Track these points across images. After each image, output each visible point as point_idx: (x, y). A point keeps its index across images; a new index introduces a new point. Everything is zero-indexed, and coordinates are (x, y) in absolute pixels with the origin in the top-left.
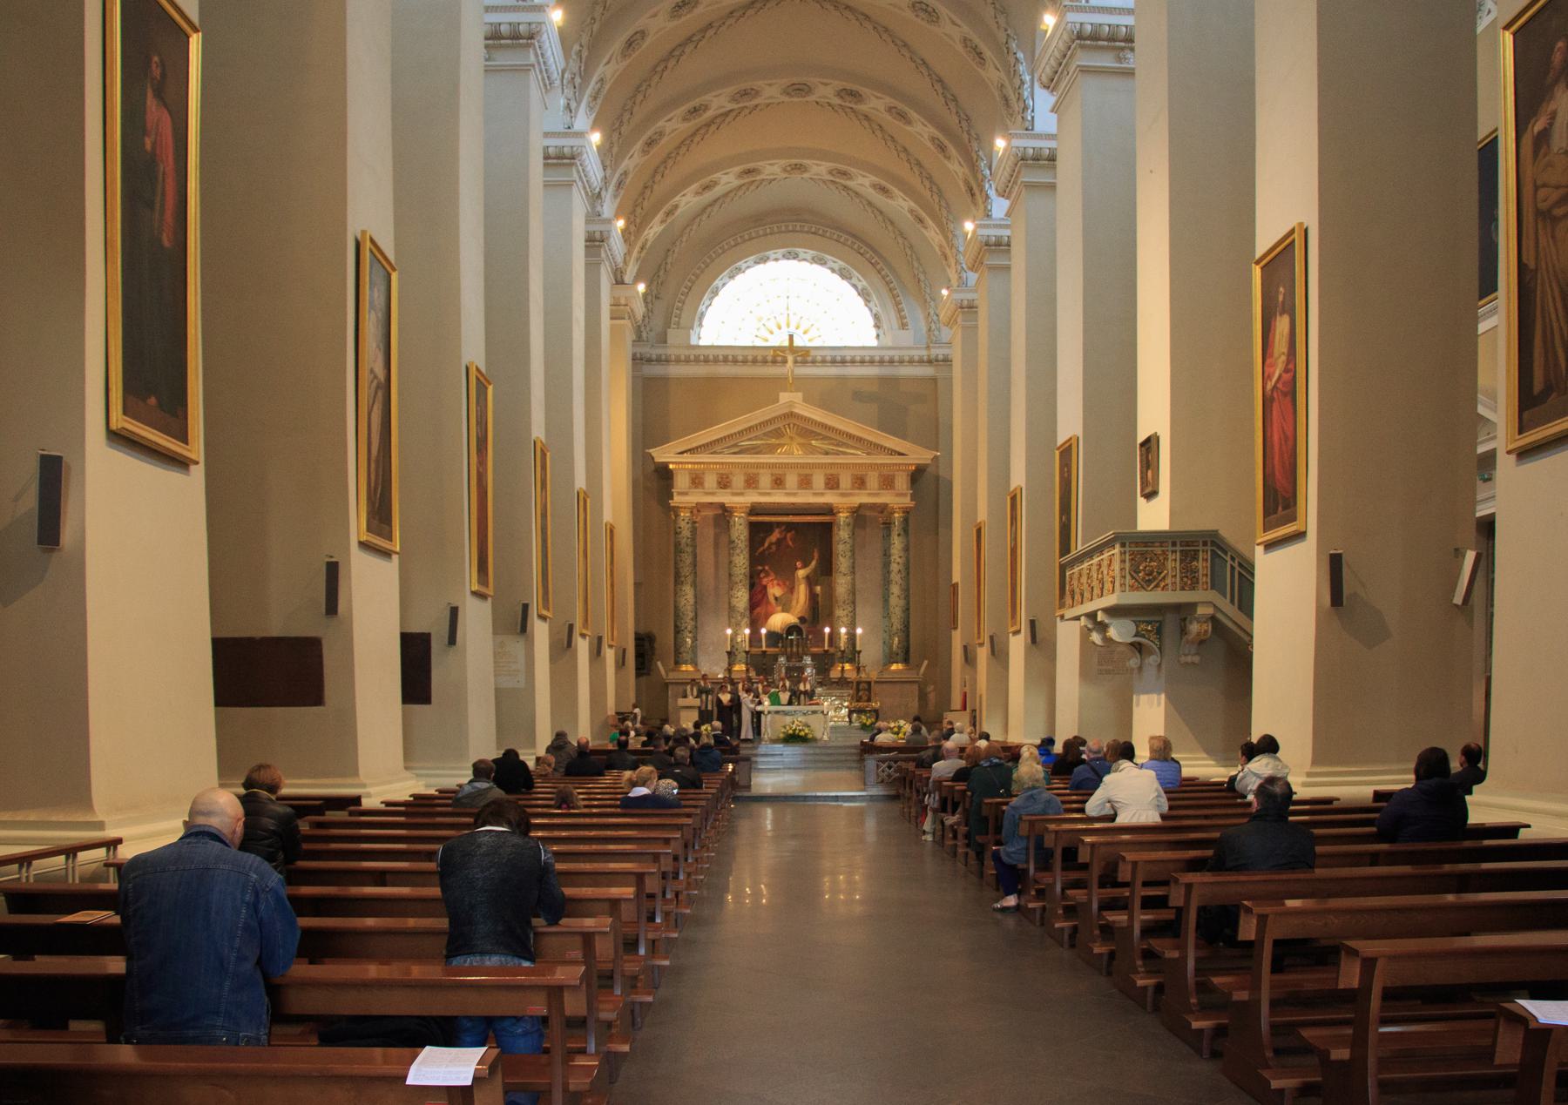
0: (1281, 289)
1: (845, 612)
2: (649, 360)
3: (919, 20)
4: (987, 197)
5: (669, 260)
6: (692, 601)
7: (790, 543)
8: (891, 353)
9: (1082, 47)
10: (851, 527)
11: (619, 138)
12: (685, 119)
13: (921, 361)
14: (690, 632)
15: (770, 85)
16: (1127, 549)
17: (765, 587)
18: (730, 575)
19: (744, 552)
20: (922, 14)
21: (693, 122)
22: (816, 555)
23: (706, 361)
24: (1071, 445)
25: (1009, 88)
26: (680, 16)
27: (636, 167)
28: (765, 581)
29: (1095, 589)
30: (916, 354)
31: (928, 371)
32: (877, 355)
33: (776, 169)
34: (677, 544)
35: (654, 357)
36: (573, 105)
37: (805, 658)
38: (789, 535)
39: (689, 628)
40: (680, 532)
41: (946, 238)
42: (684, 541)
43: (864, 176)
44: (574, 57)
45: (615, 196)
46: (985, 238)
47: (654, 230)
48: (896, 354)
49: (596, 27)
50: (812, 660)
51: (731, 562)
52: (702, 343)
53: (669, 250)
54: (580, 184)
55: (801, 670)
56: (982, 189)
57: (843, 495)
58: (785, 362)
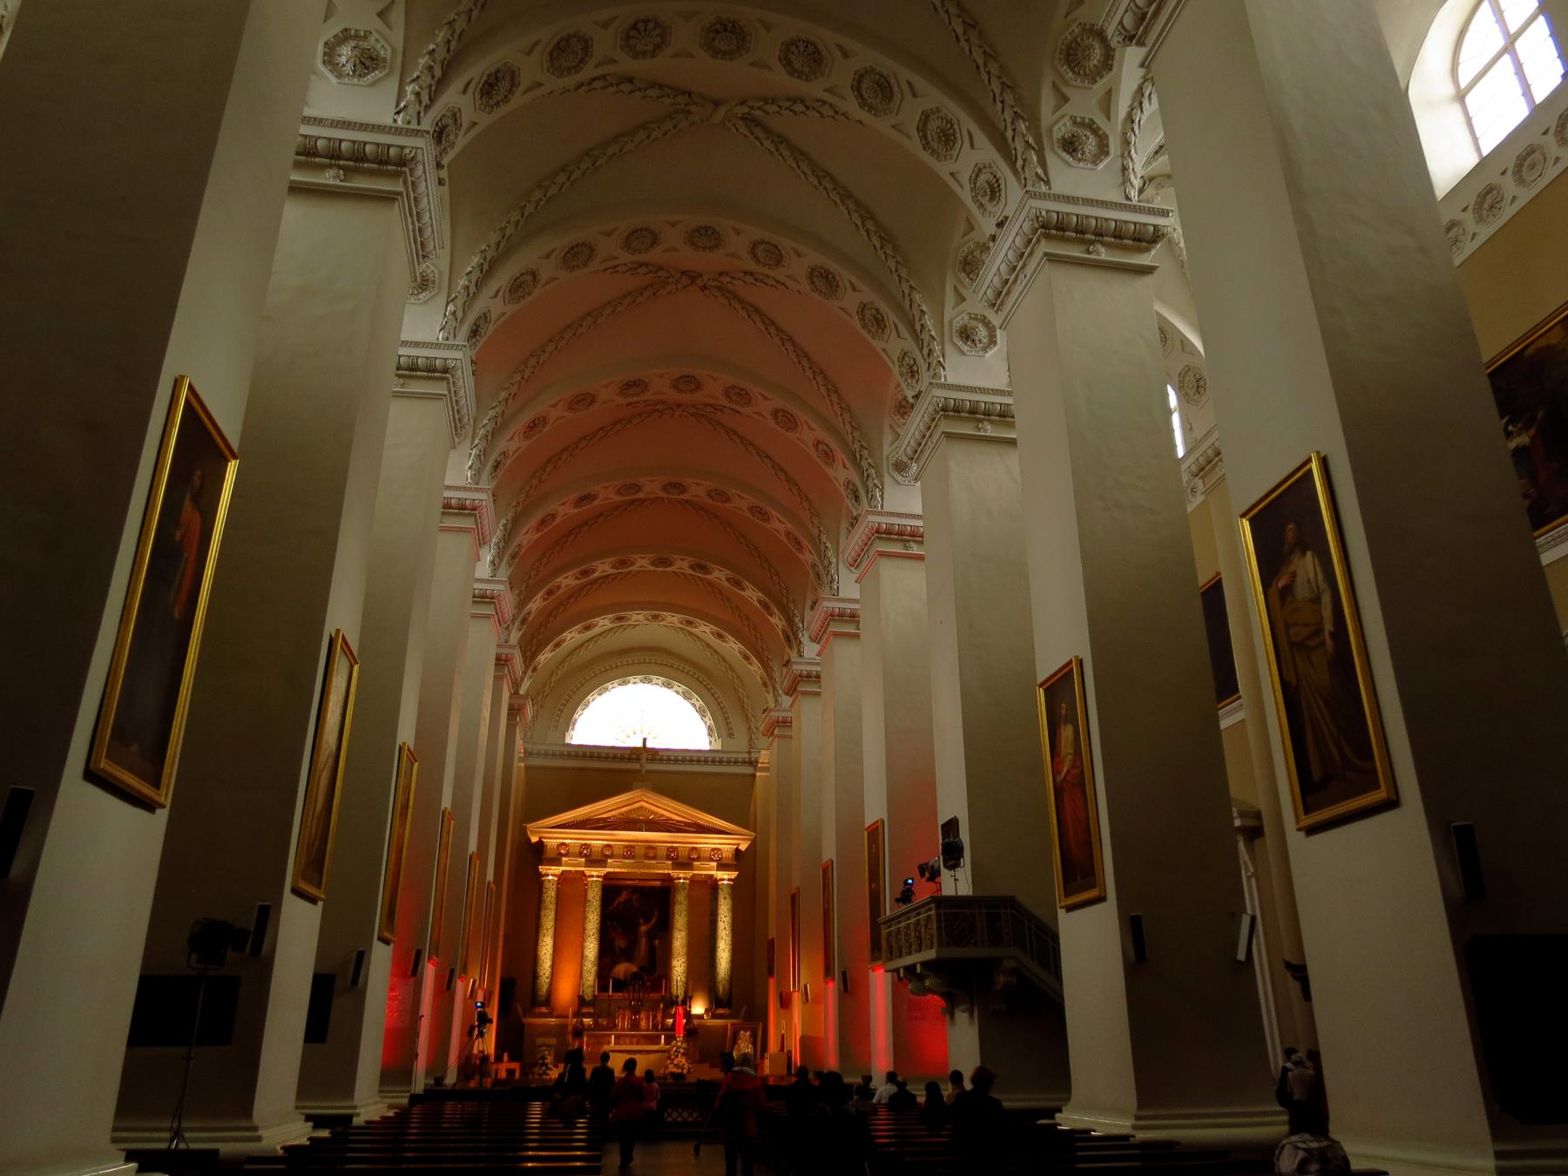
0: (1063, 705)
2: (531, 754)
3: (755, 518)
4: (801, 643)
5: (553, 680)
8: (721, 755)
9: (880, 538)
10: (686, 891)
11: (526, 588)
12: (577, 578)
13: (744, 762)
15: (642, 558)
16: (942, 911)
20: (757, 515)
21: (582, 581)
22: (656, 914)
24: (878, 826)
25: (820, 567)
26: (581, 507)
27: (537, 609)
29: (913, 944)
30: (741, 756)
32: (710, 756)
33: (641, 617)
35: (535, 751)
36: (497, 561)
38: (634, 897)
41: (766, 672)
43: (706, 626)
44: (502, 528)
45: (520, 630)
46: (799, 672)
47: (545, 657)
48: (725, 756)
49: (519, 509)
52: (575, 742)
53: (553, 672)
54: (496, 617)
56: (796, 637)
58: (638, 760)
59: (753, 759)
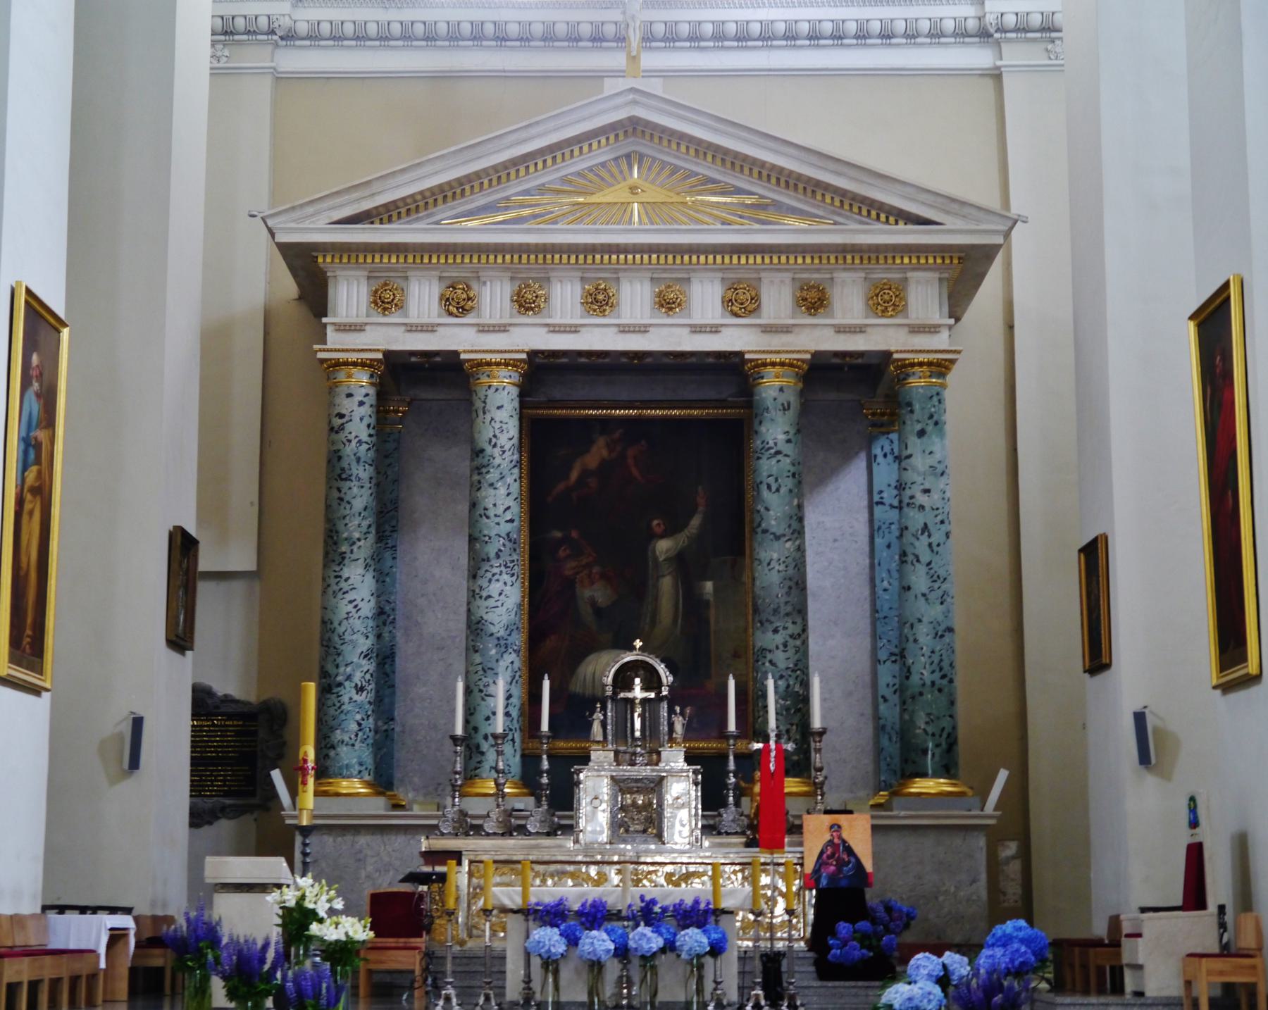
1: (779, 638)
2: (290, 36)
6: (368, 608)
7: (635, 472)
10: (791, 413)
13: (961, 34)
14: (360, 689)
17: (569, 584)
18: (472, 539)
19: (509, 480)
22: (701, 501)
23: (430, 37)
28: (569, 567)
31: (978, 57)
34: (335, 457)
35: (302, 28)
37: (666, 753)
39: (357, 678)
40: (342, 428)
42: (349, 450)
50: (689, 759)
51: (473, 505)
55: (657, 785)
57: (768, 329)
59: (990, 19)
